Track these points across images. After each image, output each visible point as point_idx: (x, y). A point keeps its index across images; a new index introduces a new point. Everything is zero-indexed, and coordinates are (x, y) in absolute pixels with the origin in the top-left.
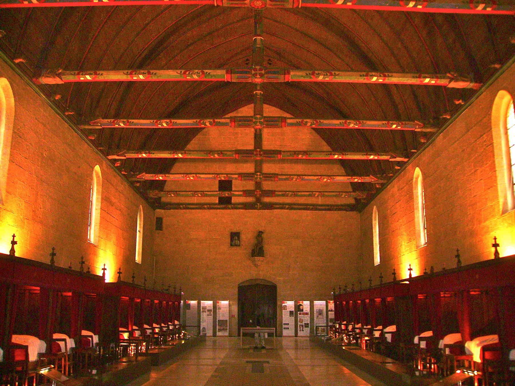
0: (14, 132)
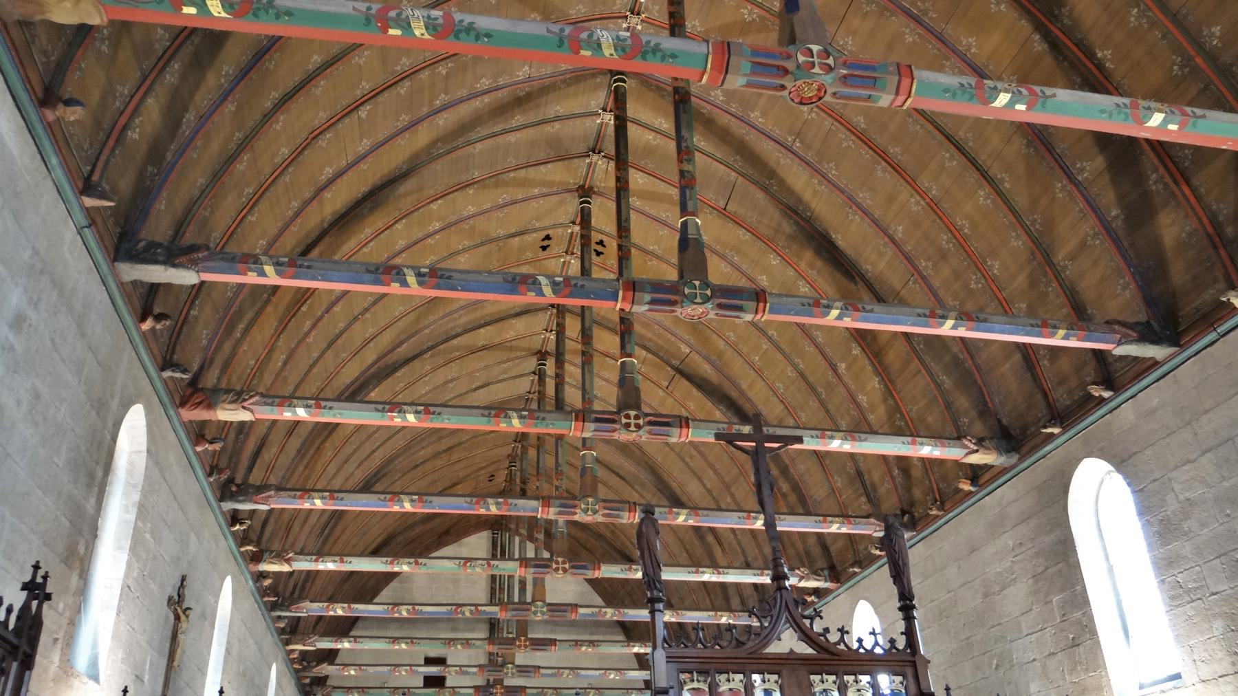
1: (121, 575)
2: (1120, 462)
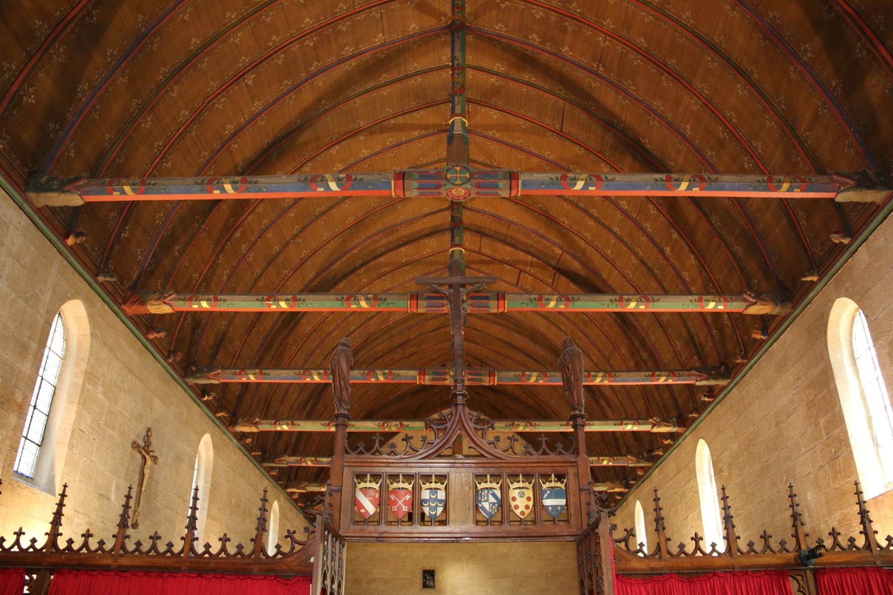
0: (212, 486)
1: (72, 422)
2: (862, 300)
